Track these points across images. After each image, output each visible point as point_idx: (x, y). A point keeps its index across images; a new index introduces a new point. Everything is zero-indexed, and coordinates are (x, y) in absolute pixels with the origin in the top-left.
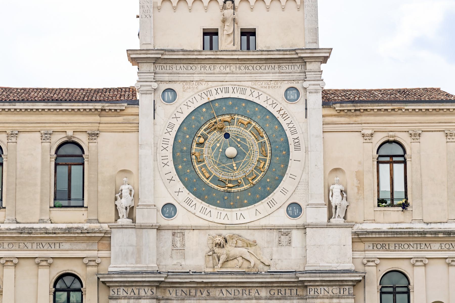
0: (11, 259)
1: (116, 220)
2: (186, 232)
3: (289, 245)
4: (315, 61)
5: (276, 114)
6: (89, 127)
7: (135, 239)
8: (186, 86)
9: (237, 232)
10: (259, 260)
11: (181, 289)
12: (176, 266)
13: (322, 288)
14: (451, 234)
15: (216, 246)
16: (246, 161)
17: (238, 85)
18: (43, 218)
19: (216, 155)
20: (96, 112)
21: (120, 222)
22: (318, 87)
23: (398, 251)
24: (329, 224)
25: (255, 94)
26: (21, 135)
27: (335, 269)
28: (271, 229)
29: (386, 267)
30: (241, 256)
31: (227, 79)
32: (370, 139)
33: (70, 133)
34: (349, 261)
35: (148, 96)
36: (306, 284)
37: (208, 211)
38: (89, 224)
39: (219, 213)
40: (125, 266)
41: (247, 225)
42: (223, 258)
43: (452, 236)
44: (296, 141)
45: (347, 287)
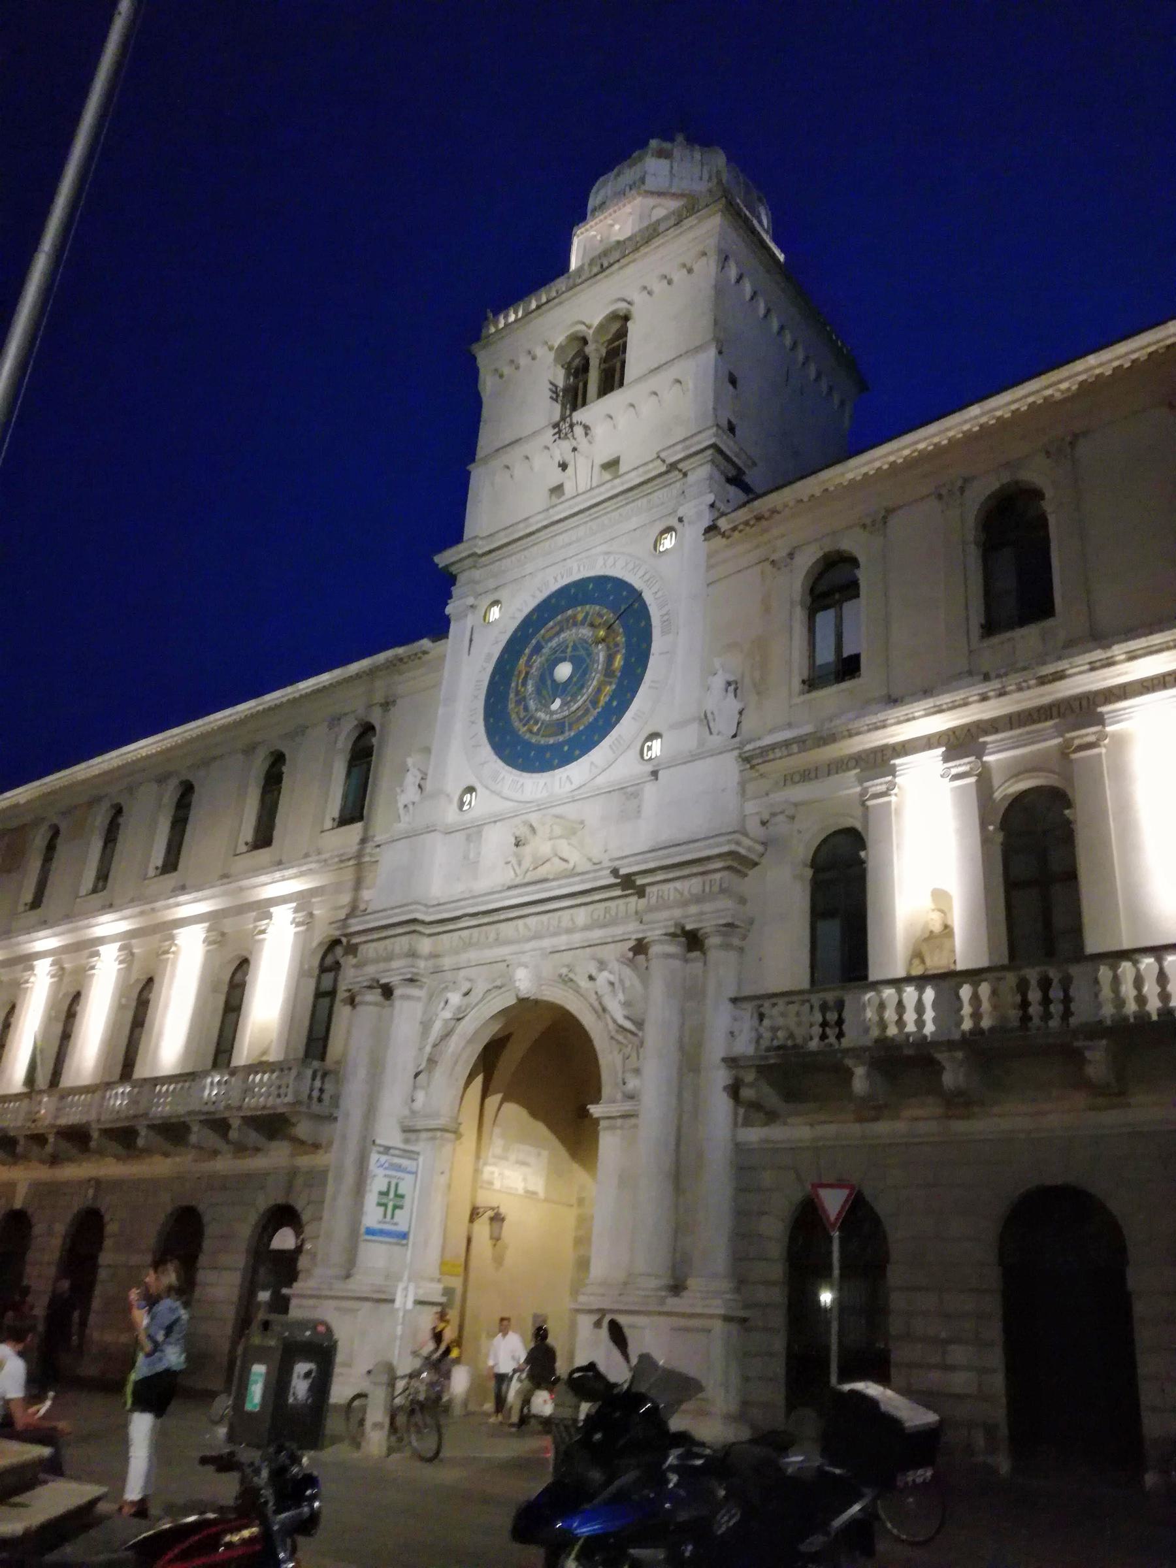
25: (611, 560)
36: (640, 881)
37: (520, 784)
44: (666, 618)
45: (718, 876)
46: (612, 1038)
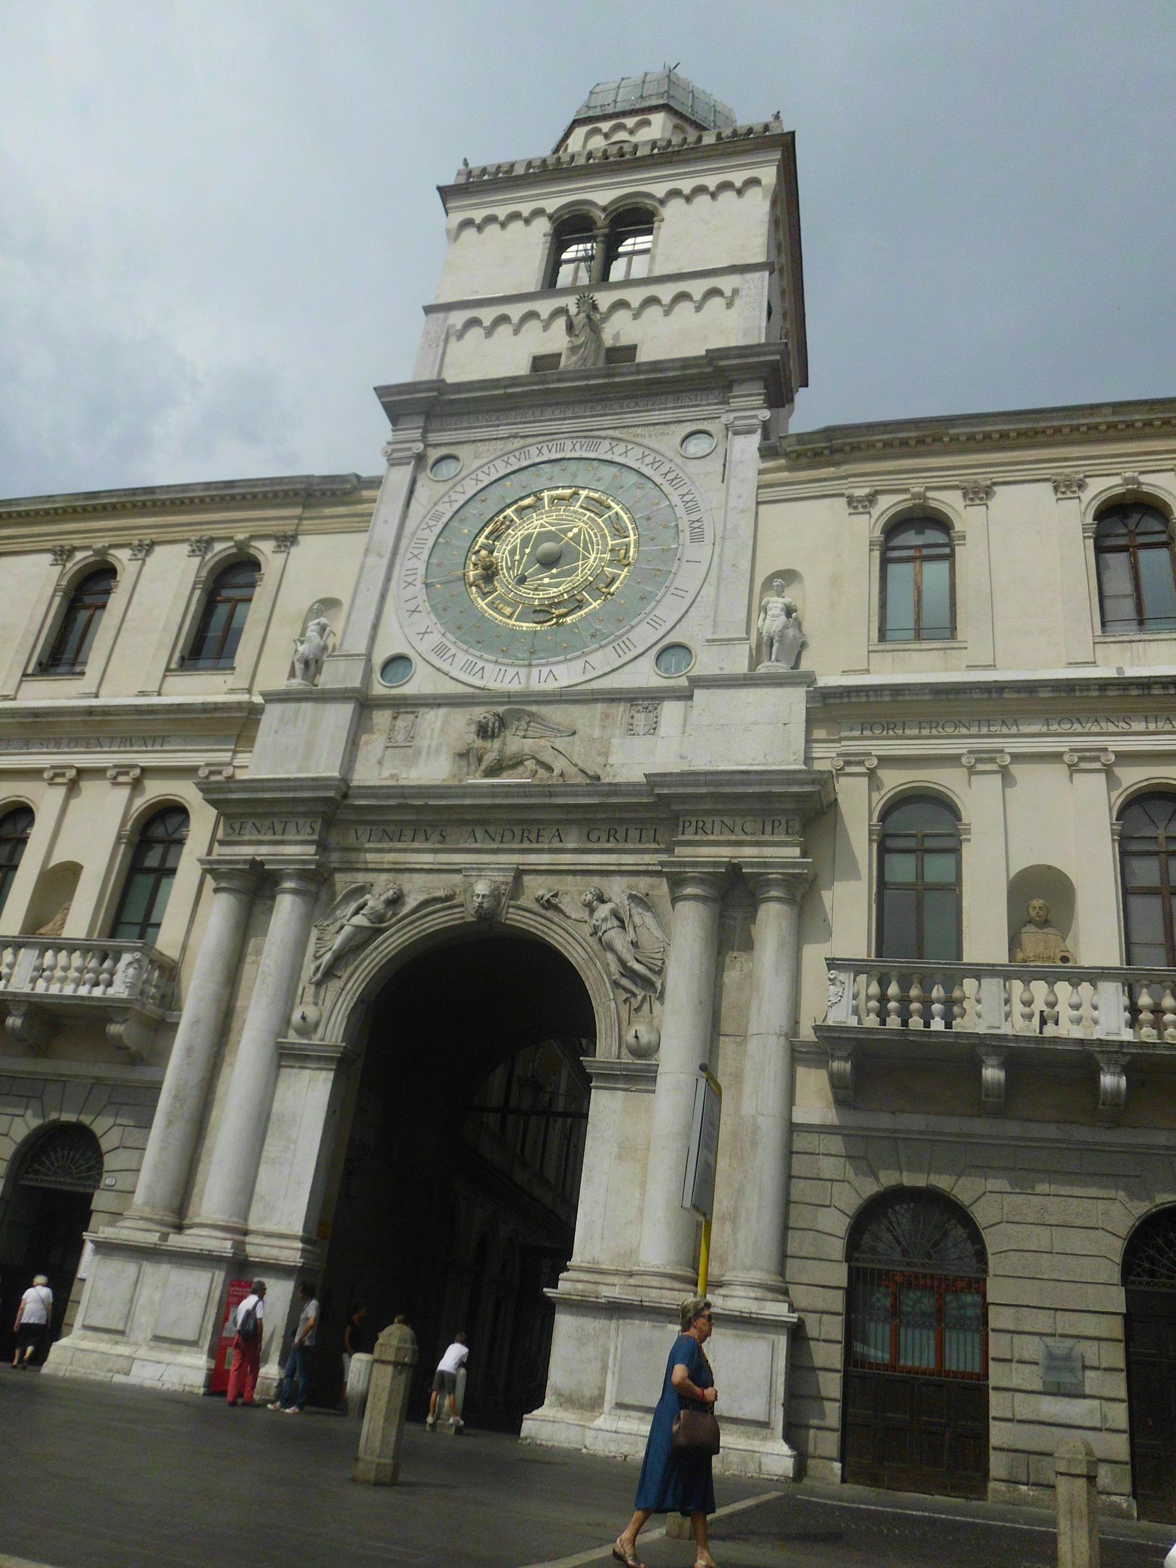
2: (422, 710)
3: (652, 731)
6: (279, 525)
8: (481, 448)
9: (533, 708)
10: (575, 765)
11: (382, 827)
13: (717, 819)
14: (1074, 690)
17: (585, 437)
22: (755, 421)
26: (158, 550)
29: (894, 780)
30: (534, 758)
31: (564, 428)
33: (241, 537)
34: (795, 760)
35: (404, 467)
36: (675, 807)
42: (489, 758)
43: (1078, 694)
44: (696, 525)
46: (616, 984)
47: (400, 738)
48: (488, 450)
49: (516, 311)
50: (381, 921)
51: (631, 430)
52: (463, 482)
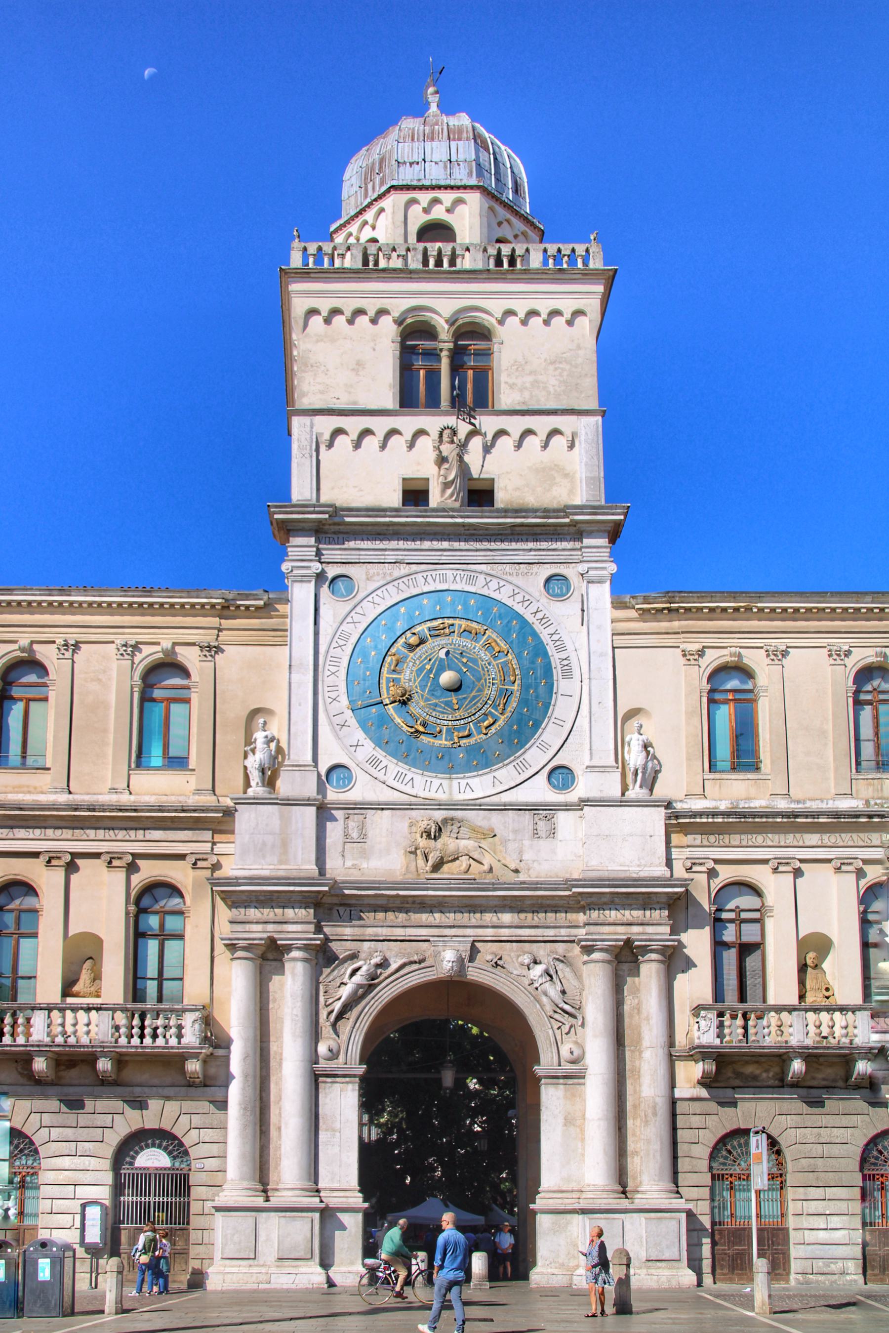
0: (59, 855)
1: (245, 792)
4: (598, 531)
5: (530, 618)
7: (278, 822)
9: (458, 814)
12: (352, 871)
15: (422, 837)
16: (474, 697)
18: (116, 786)
19: (424, 683)
20: (213, 612)
21: (251, 792)
23: (747, 847)
24: (624, 799)
27: (635, 875)
28: (520, 808)
31: (444, 559)
32: (695, 660)
35: (305, 585)
38: (197, 797)
39: (429, 783)
40: (260, 867)
41: (478, 802)
44: (565, 662)
47: (355, 835)
48: (378, 574)
49: (380, 425)
50: (373, 979)
51: (500, 567)
52: (362, 604)
